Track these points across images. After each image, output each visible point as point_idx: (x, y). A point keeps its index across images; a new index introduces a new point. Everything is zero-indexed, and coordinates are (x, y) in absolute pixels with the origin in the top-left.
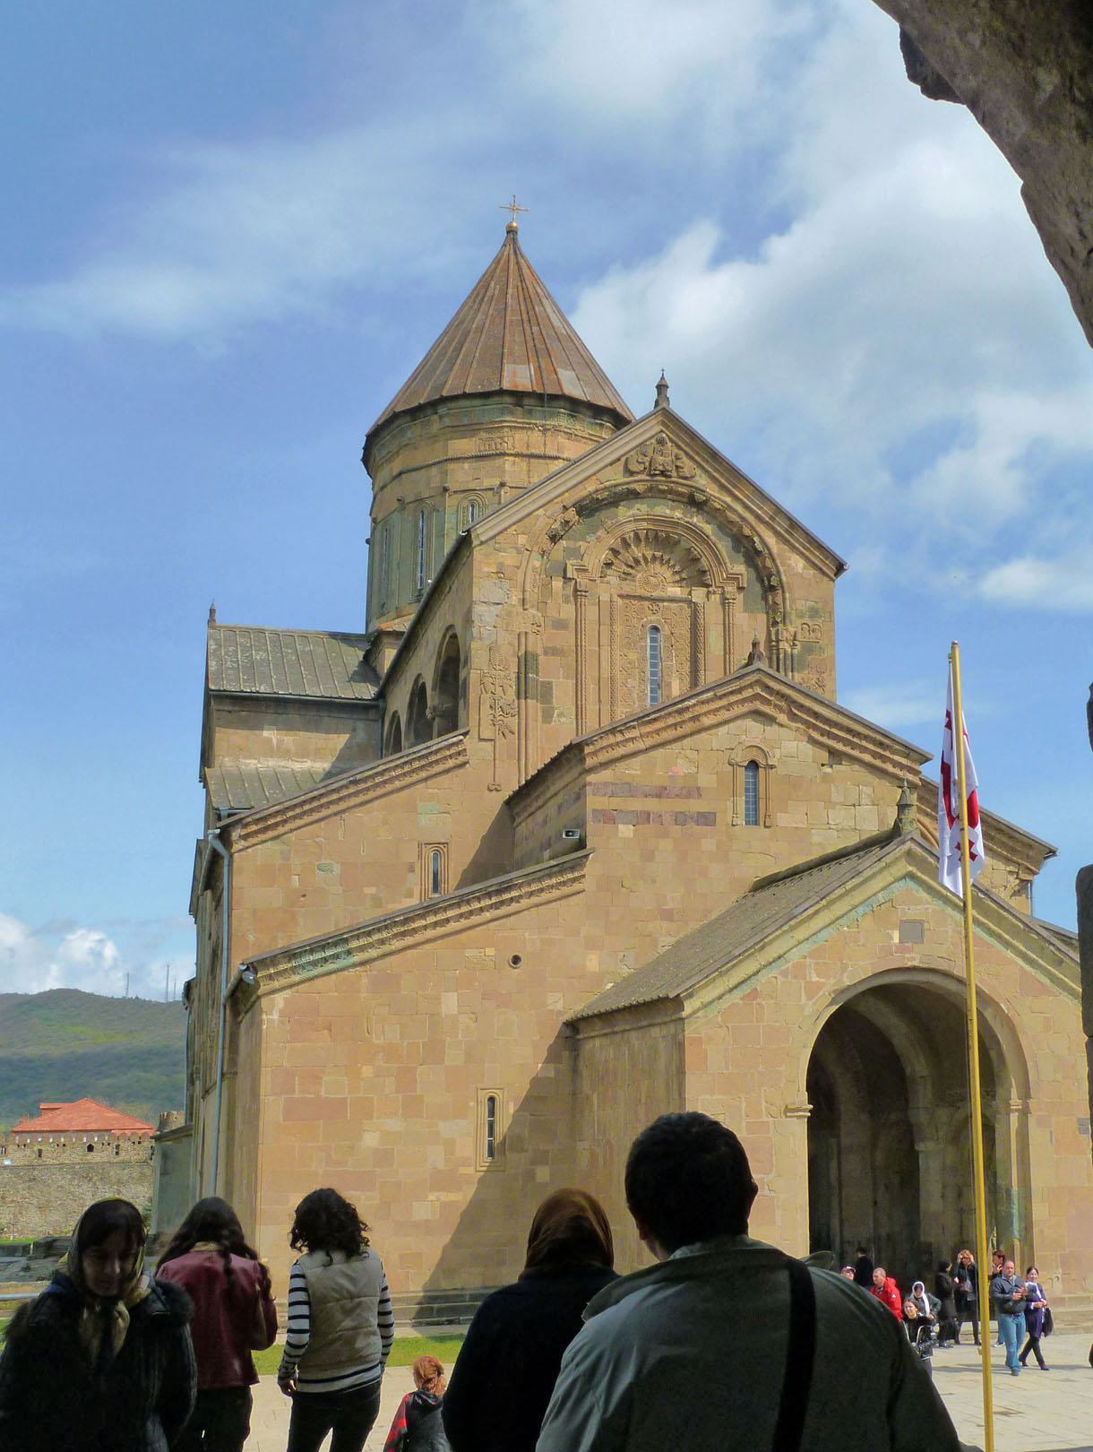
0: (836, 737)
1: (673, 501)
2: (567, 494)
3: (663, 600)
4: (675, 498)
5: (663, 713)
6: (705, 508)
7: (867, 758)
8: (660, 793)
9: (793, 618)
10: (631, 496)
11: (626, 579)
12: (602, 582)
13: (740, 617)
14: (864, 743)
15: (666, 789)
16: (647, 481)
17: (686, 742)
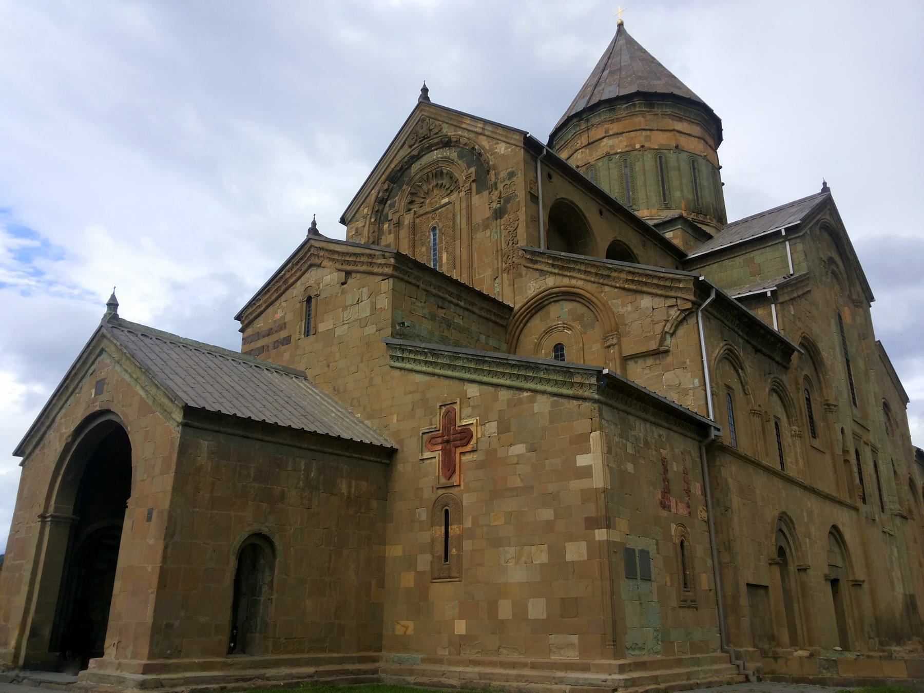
0: (348, 263)
1: (436, 150)
2: (383, 176)
3: (438, 209)
4: (435, 147)
5: (270, 286)
6: (452, 144)
7: (364, 268)
8: (269, 333)
9: (498, 185)
10: (415, 159)
11: (421, 207)
12: (406, 215)
13: (476, 199)
14: (362, 259)
15: (272, 329)
16: (418, 147)
17: (283, 298)
